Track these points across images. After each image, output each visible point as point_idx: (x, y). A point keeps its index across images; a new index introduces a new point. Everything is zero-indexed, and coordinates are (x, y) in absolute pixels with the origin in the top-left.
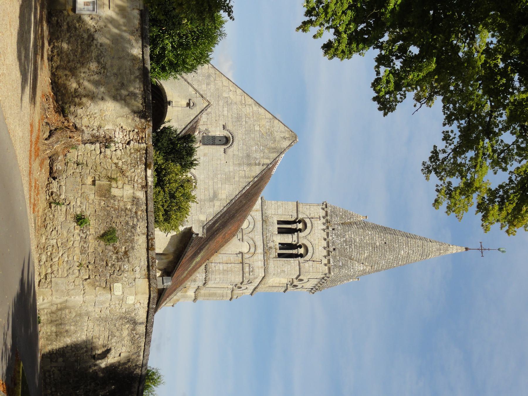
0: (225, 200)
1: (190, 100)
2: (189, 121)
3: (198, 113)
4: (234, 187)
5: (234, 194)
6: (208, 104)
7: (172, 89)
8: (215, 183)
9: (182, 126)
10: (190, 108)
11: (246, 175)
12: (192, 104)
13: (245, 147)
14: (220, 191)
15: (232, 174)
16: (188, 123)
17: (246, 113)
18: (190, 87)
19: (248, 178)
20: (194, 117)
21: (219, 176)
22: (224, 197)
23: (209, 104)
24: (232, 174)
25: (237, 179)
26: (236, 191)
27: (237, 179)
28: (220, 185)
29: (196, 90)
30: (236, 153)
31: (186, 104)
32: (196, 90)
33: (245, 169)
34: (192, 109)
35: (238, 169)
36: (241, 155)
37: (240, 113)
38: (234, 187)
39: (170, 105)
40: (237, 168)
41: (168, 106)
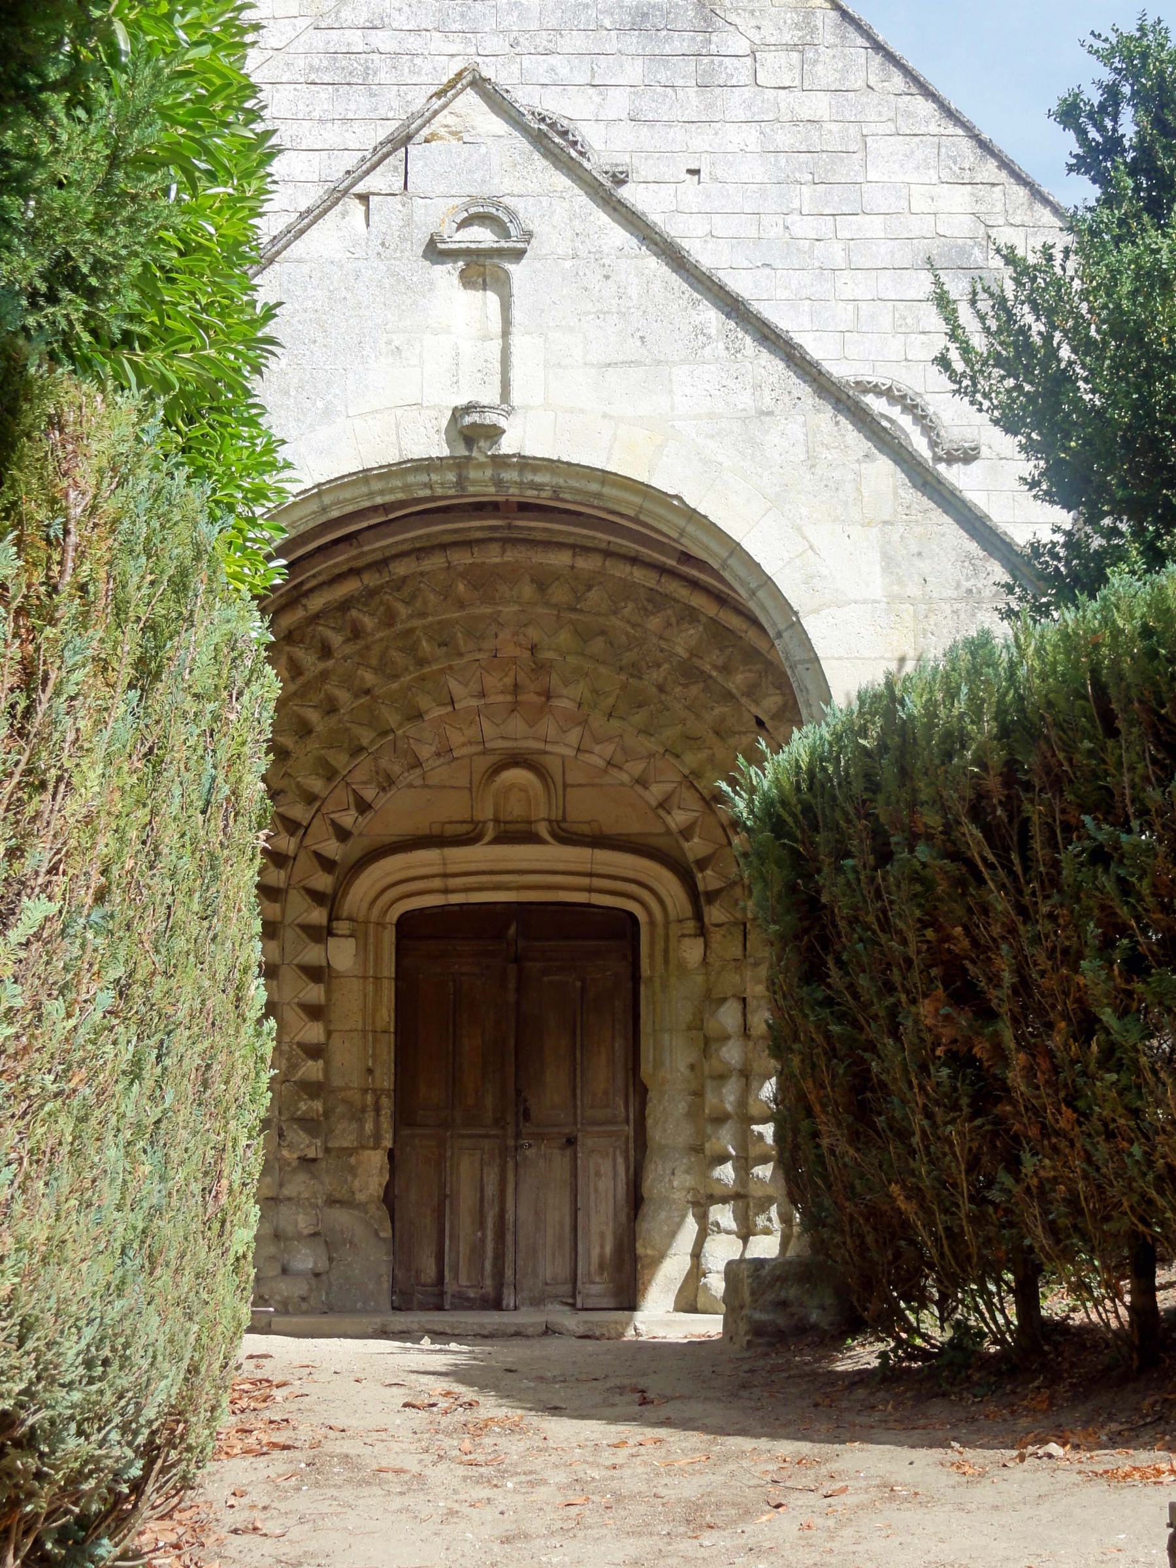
0: (982, 191)
1: (435, 252)
2: (654, 265)
3: (561, 181)
4: (882, 128)
5: (933, 129)
6: (470, 98)
7: (328, 413)
8: (858, 261)
9: (700, 331)
10: (518, 255)
11: (787, 38)
12: (483, 237)
13: (575, 41)
14: (919, 226)
15: (784, 138)
16: (675, 280)
17: (302, 23)
18: (298, 248)
19: (813, 30)
20: (601, 218)
21: (803, 227)
22: (958, 199)
23: (473, 84)
24: (784, 138)
25: (819, 105)
26: (909, 115)
27: (819, 105)
28: (874, 226)
29: (336, 196)
30: (618, 103)
31: (475, 296)
32: (336, 196)
33: (743, 47)
34: (528, 235)
35: (747, 93)
36: (634, 71)
37: (301, 62)
38: (882, 128)
39: (494, 433)
40: (736, 103)
41: (507, 446)
